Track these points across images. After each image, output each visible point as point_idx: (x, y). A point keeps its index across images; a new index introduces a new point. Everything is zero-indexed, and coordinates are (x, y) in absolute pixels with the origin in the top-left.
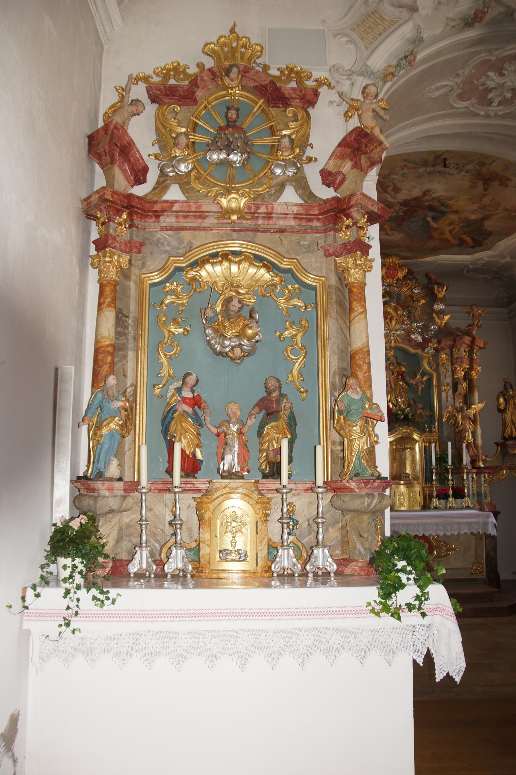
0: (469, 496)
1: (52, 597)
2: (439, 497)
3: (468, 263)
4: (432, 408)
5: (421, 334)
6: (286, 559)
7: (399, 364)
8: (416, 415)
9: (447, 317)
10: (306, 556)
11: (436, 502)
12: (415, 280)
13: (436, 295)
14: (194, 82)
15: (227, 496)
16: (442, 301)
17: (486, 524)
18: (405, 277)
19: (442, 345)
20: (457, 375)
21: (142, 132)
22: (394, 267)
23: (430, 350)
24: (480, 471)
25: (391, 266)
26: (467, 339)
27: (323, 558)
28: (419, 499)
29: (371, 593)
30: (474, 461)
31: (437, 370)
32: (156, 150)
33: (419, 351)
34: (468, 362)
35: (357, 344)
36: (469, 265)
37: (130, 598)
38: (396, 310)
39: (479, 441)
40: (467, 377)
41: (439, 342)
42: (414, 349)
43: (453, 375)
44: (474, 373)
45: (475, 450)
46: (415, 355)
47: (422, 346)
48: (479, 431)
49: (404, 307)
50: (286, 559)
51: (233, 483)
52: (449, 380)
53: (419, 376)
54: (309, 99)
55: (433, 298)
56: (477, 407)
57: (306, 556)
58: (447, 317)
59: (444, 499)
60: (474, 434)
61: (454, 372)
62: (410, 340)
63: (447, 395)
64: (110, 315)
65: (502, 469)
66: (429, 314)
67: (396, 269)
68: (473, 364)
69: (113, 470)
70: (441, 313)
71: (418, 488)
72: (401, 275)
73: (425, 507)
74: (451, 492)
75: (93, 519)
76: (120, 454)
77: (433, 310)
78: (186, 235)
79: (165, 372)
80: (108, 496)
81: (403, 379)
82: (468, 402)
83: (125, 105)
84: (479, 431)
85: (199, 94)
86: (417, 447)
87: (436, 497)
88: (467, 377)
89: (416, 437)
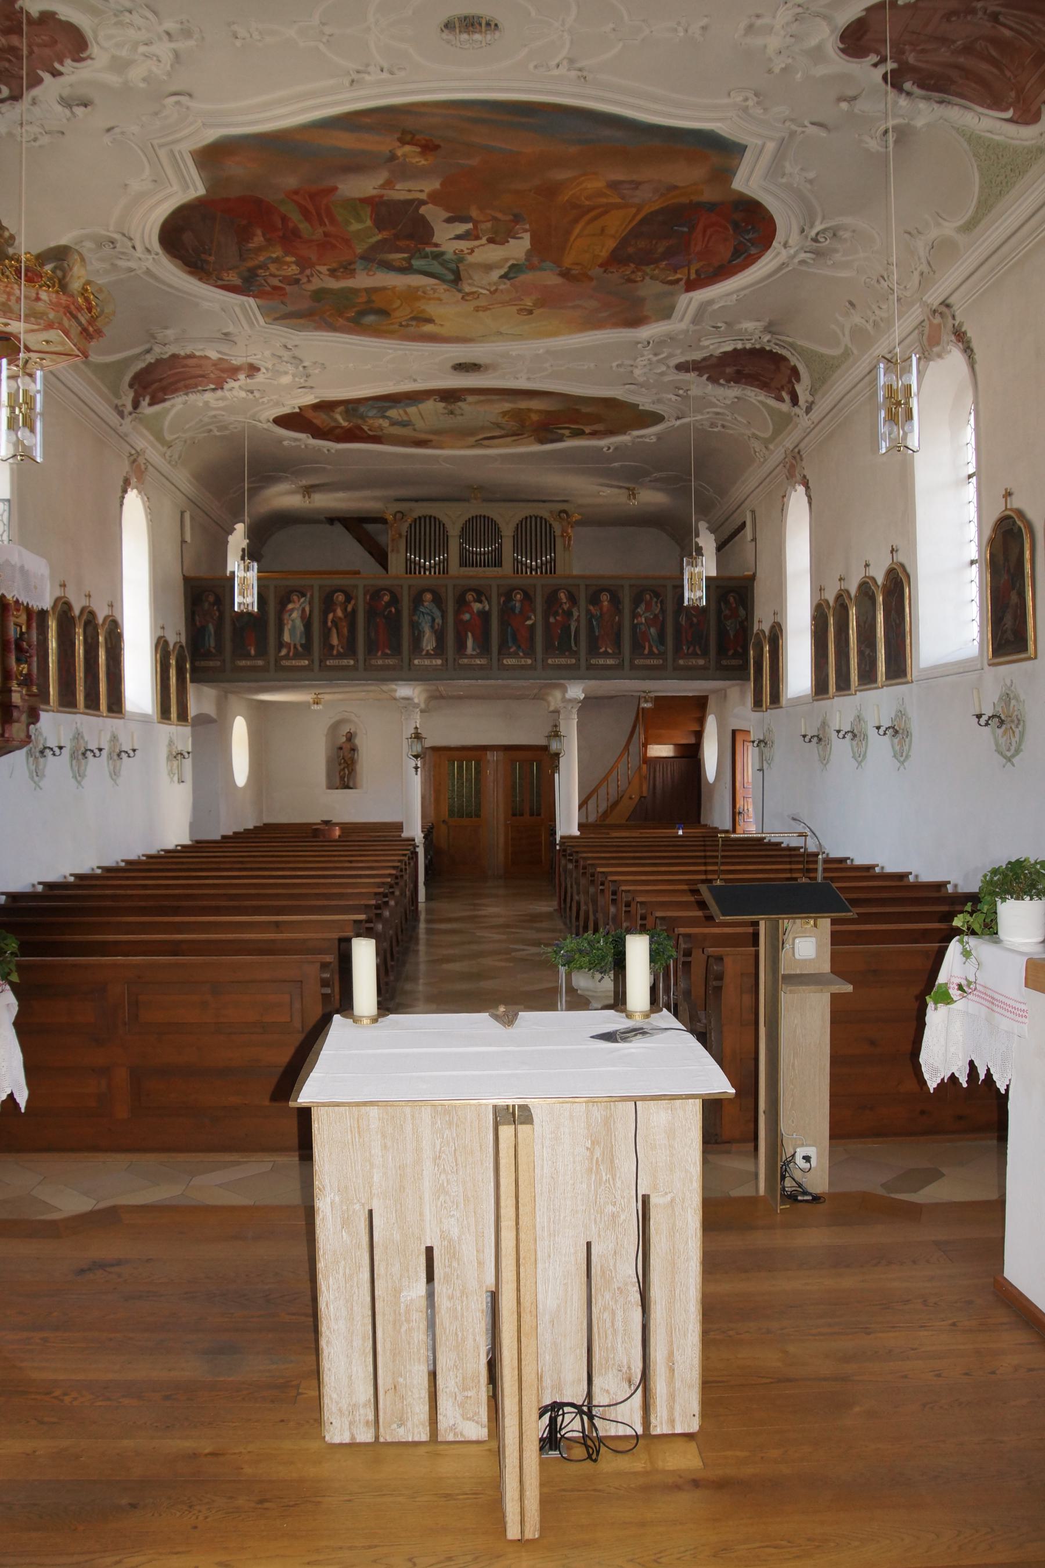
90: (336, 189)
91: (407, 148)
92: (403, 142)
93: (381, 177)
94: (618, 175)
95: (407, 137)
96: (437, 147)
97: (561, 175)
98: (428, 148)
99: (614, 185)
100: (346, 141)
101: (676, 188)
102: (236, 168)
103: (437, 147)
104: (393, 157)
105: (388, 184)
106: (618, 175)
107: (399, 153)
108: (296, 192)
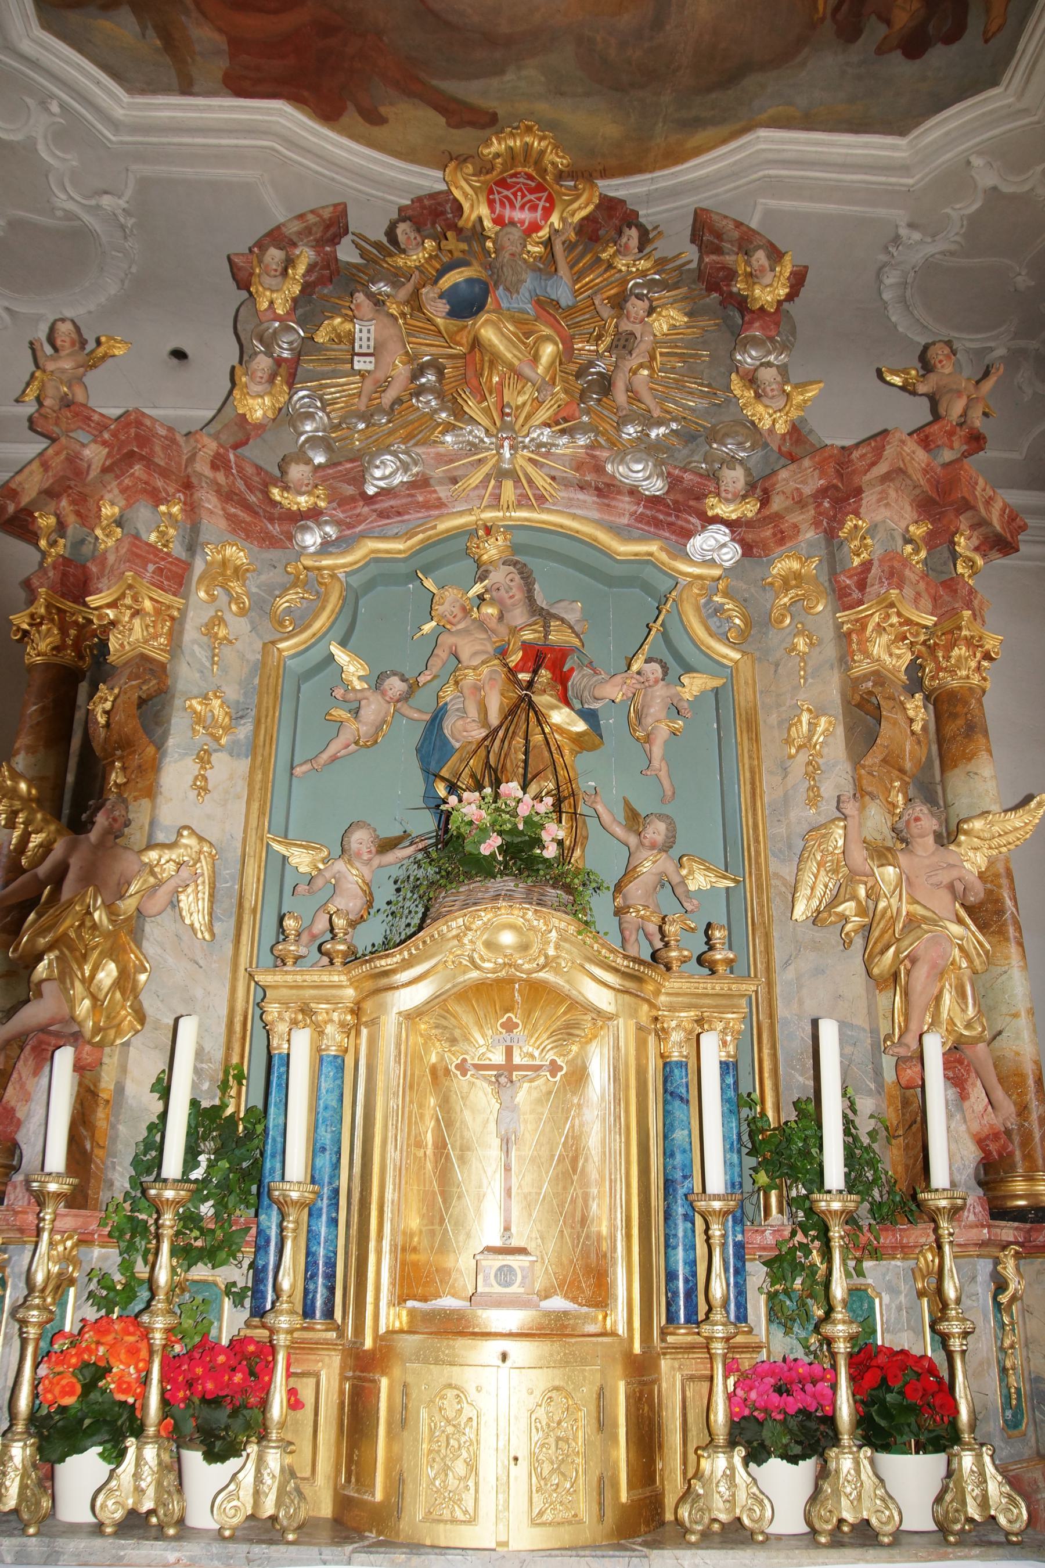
2: (752, 1438)
3: (899, 216)
8: (635, 890)
12: (634, 233)
13: (742, 304)
19: (777, 504)
20: (867, 655)
22: (530, 177)
23: (714, 546)
25: (515, 175)
34: (926, 602)
36: (903, 232)
41: (760, 488)
42: (629, 539)
43: (845, 660)
45: (999, 1094)
46: (637, 578)
59: (793, 1460)
62: (608, 491)
67: (540, 188)
68: (955, 613)
74: (845, 1410)
77: (735, 367)
84: (1017, 984)
87: (732, 1444)
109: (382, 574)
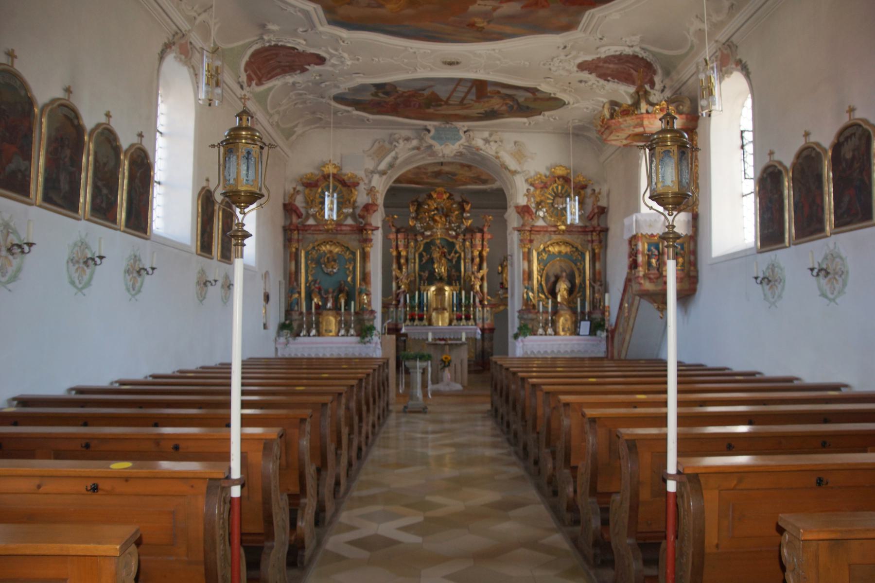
0: (475, 319)
1: (282, 340)
4: (460, 272)
5: (455, 231)
6: (343, 332)
7: (443, 247)
9: (470, 221)
10: (347, 331)
11: (455, 322)
14: (318, 181)
15: (327, 315)
16: (468, 212)
17: (475, 333)
18: (448, 198)
21: (299, 202)
24: (483, 306)
26: (479, 235)
27: (352, 332)
28: (447, 321)
29: (358, 339)
30: (481, 302)
31: (464, 251)
32: (304, 205)
33: (454, 240)
35: (367, 270)
37: (300, 339)
38: (441, 218)
39: (485, 290)
40: (481, 256)
44: (485, 254)
47: (456, 237)
48: (485, 284)
49: (446, 216)
50: (343, 332)
51: (330, 312)
52: (469, 256)
53: (452, 254)
54: (356, 185)
55: (463, 210)
56: (485, 271)
57: (347, 331)
58: (470, 221)
60: (481, 287)
61: (472, 252)
63: (469, 265)
64: (293, 263)
65: (500, 305)
66: (461, 218)
69: (296, 308)
70: (468, 218)
71: (447, 315)
72: (445, 196)
73: (450, 324)
75: (291, 321)
76: (297, 304)
78: (316, 236)
79: (310, 278)
80: (295, 316)
81: (445, 256)
82: (480, 268)
83: (296, 192)
84: (485, 284)
85: (319, 184)
86: (447, 293)
88: (481, 256)
89: (447, 288)
90: (522, 8)
91: (481, 25)
92: (483, 28)
93: (499, 12)
94: (381, 11)
95: (481, 30)
96: (468, 25)
97: (409, 11)
98: (472, 25)
99: (381, 6)
100: (508, 29)
101: (349, 4)
102: (564, 20)
103: (468, 25)
104: (489, 22)
105: (495, 9)
106: (381, 11)
107: (485, 24)
108: (543, 7)
109: (427, 243)
